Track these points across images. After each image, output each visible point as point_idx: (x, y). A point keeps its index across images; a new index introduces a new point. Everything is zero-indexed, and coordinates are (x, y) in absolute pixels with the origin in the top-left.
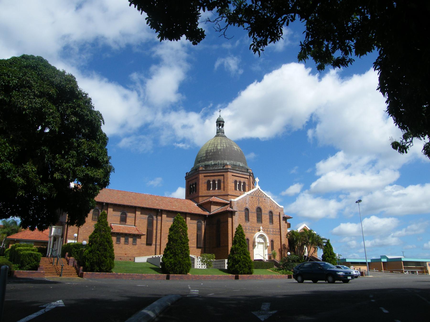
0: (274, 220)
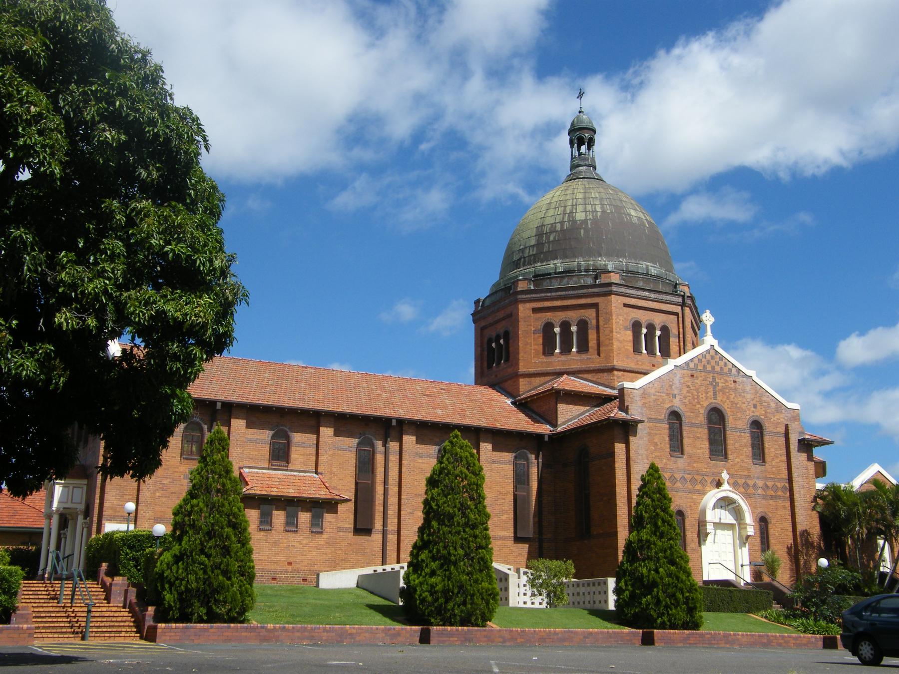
0: (766, 451)
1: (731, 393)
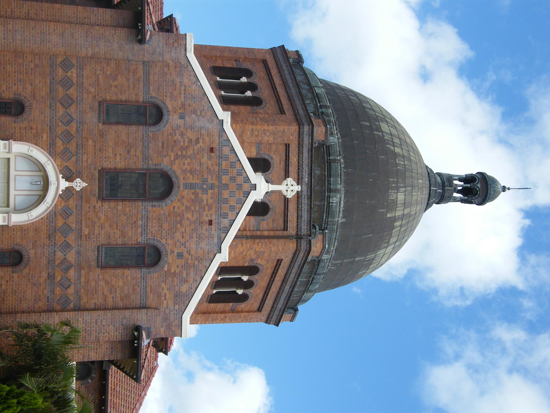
0: (119, 271)
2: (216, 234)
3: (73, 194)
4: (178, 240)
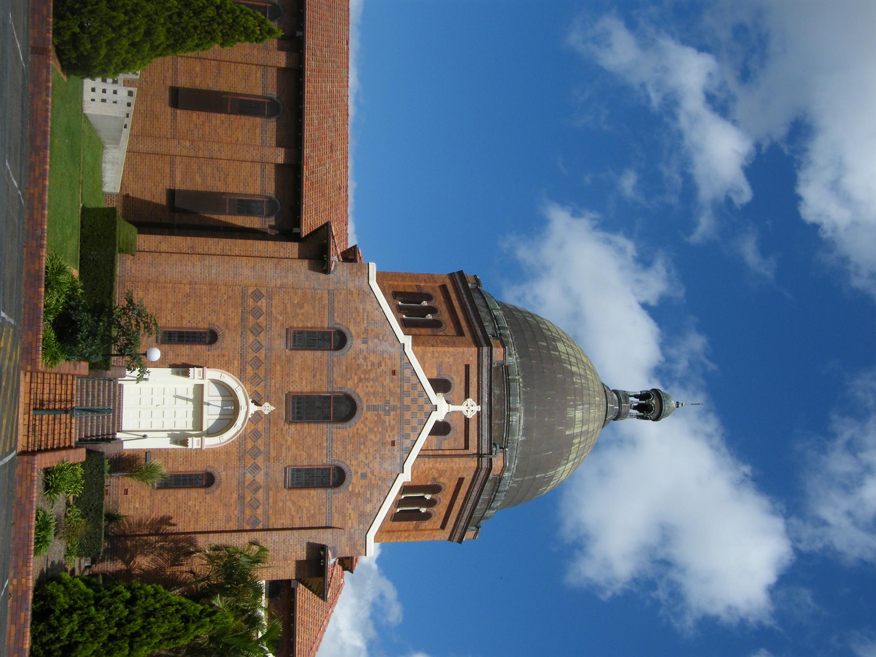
0: (305, 492)
1: (378, 434)
2: (398, 455)
3: (262, 418)
4: (362, 461)
